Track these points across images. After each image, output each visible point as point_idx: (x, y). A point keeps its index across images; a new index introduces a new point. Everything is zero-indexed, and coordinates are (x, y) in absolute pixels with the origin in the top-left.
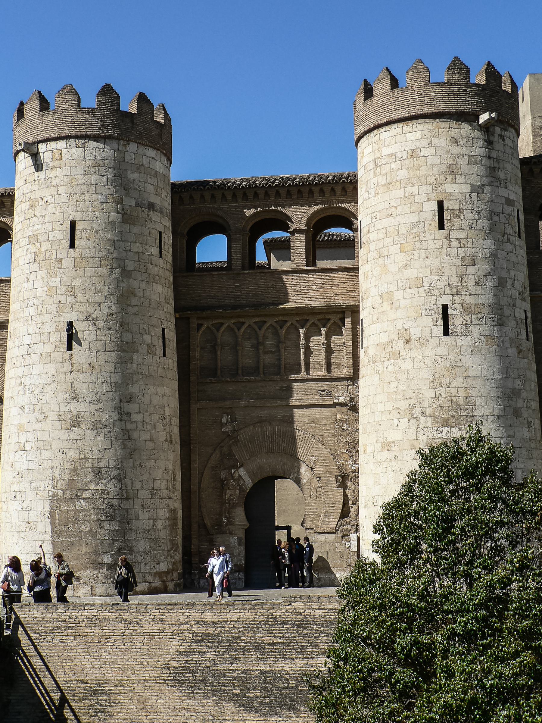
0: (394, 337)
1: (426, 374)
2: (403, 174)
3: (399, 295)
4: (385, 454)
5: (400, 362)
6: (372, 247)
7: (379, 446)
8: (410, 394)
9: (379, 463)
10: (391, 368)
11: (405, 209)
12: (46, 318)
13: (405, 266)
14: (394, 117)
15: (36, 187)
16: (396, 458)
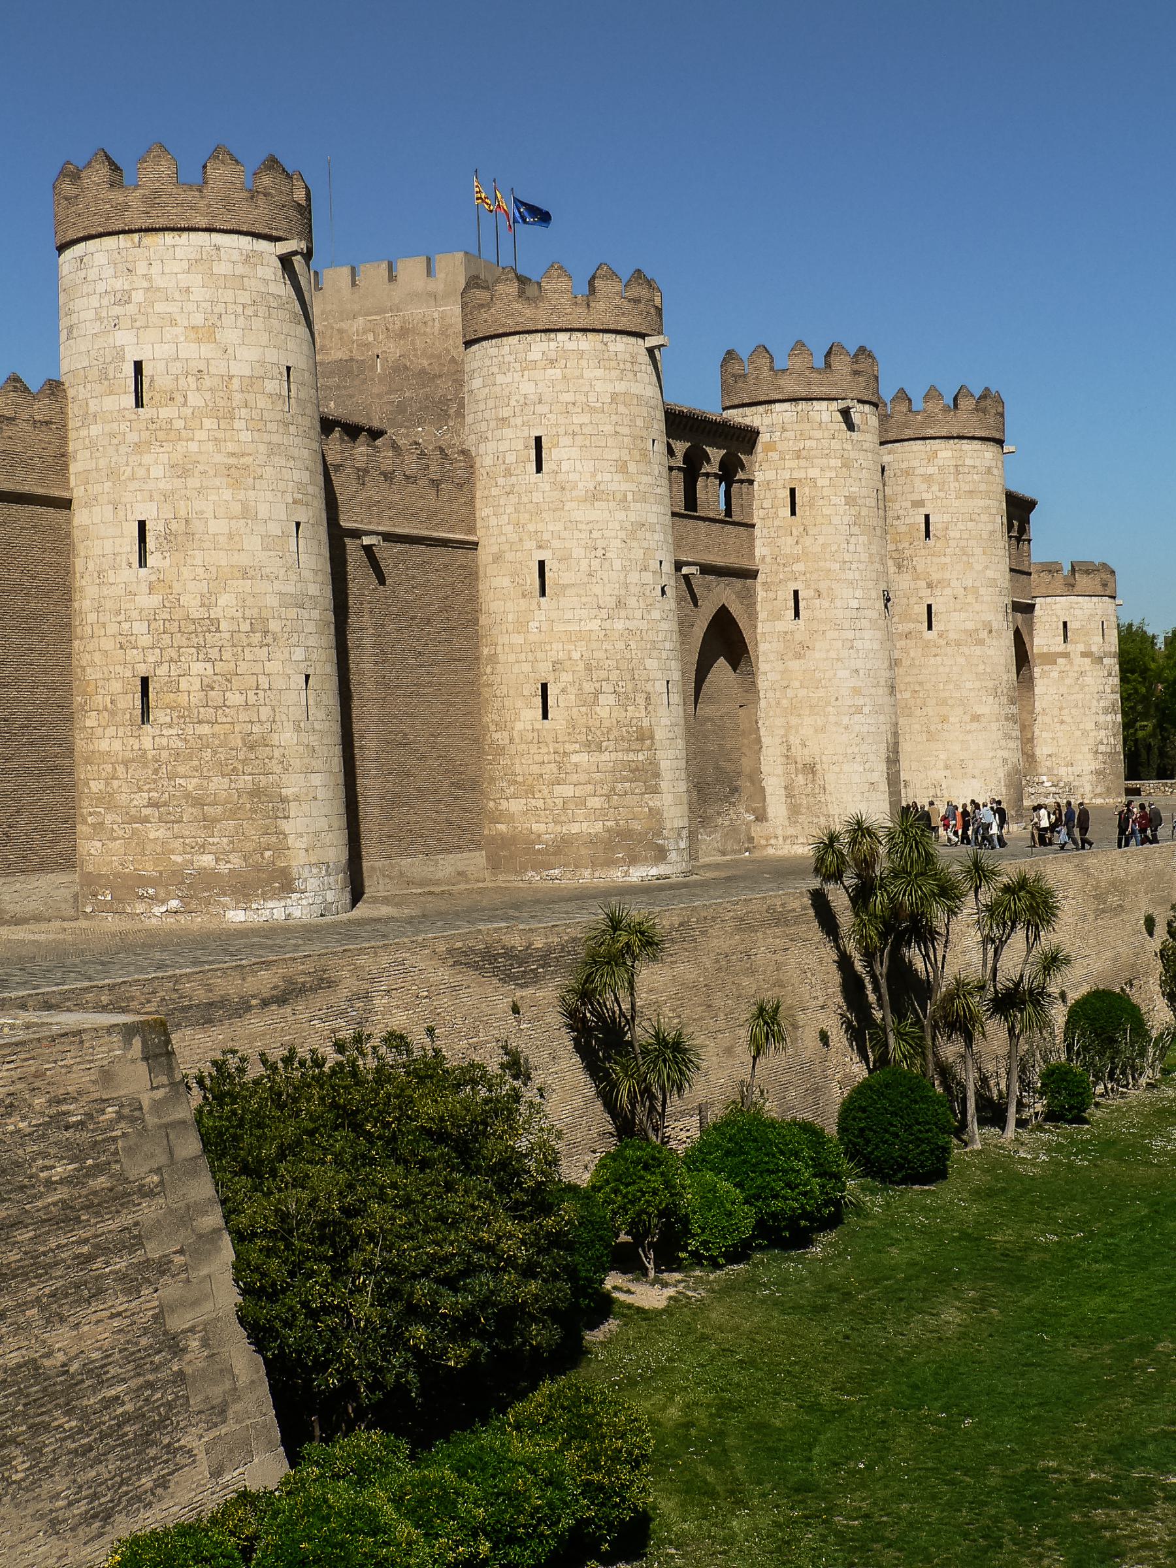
0: (980, 626)
1: (1002, 661)
2: (983, 487)
3: (982, 591)
4: (975, 725)
5: (986, 648)
6: (952, 543)
7: (967, 718)
8: (994, 676)
9: (969, 732)
10: (978, 653)
11: (984, 518)
12: (870, 584)
13: (986, 568)
14: (978, 434)
15: (849, 447)
16: (985, 728)
